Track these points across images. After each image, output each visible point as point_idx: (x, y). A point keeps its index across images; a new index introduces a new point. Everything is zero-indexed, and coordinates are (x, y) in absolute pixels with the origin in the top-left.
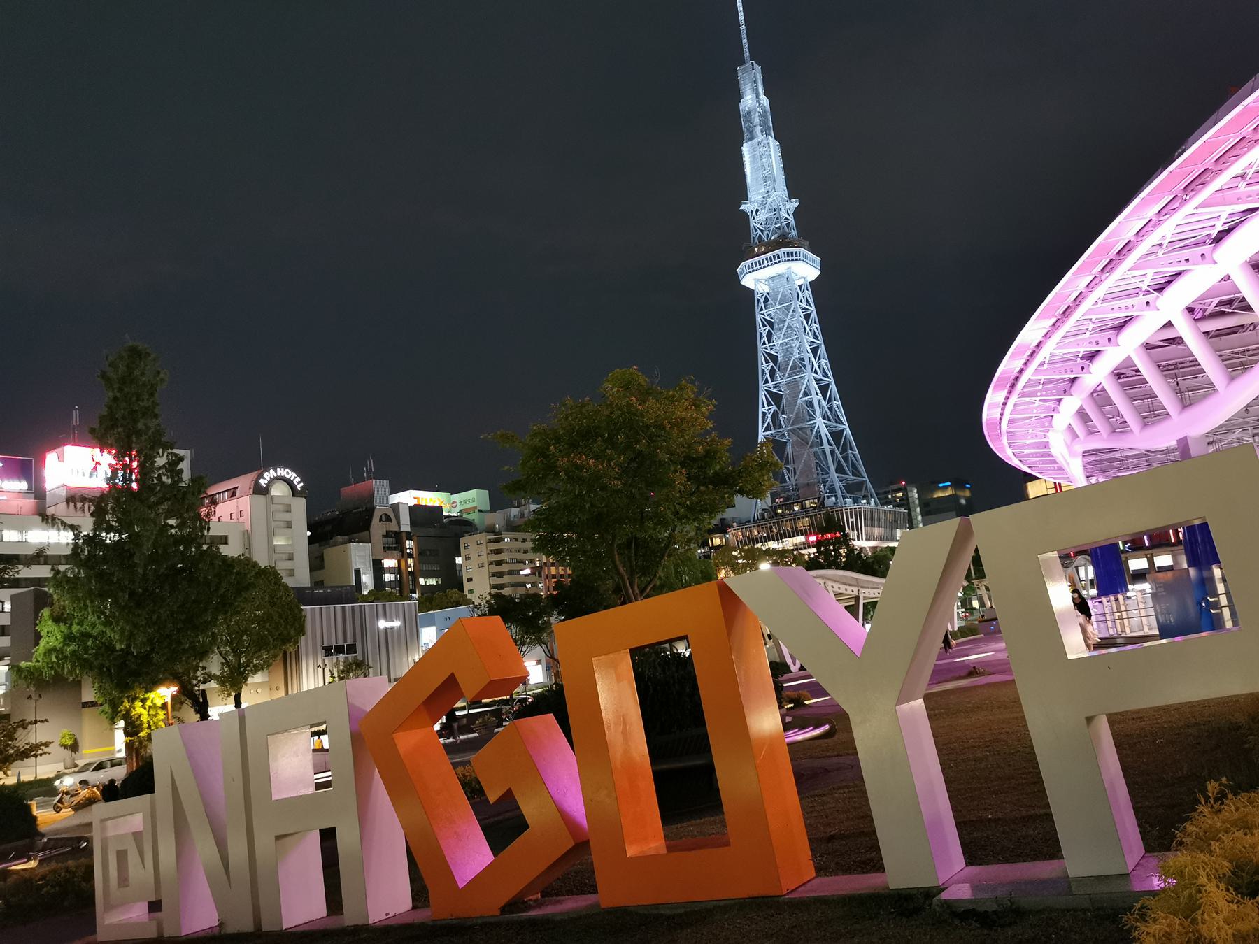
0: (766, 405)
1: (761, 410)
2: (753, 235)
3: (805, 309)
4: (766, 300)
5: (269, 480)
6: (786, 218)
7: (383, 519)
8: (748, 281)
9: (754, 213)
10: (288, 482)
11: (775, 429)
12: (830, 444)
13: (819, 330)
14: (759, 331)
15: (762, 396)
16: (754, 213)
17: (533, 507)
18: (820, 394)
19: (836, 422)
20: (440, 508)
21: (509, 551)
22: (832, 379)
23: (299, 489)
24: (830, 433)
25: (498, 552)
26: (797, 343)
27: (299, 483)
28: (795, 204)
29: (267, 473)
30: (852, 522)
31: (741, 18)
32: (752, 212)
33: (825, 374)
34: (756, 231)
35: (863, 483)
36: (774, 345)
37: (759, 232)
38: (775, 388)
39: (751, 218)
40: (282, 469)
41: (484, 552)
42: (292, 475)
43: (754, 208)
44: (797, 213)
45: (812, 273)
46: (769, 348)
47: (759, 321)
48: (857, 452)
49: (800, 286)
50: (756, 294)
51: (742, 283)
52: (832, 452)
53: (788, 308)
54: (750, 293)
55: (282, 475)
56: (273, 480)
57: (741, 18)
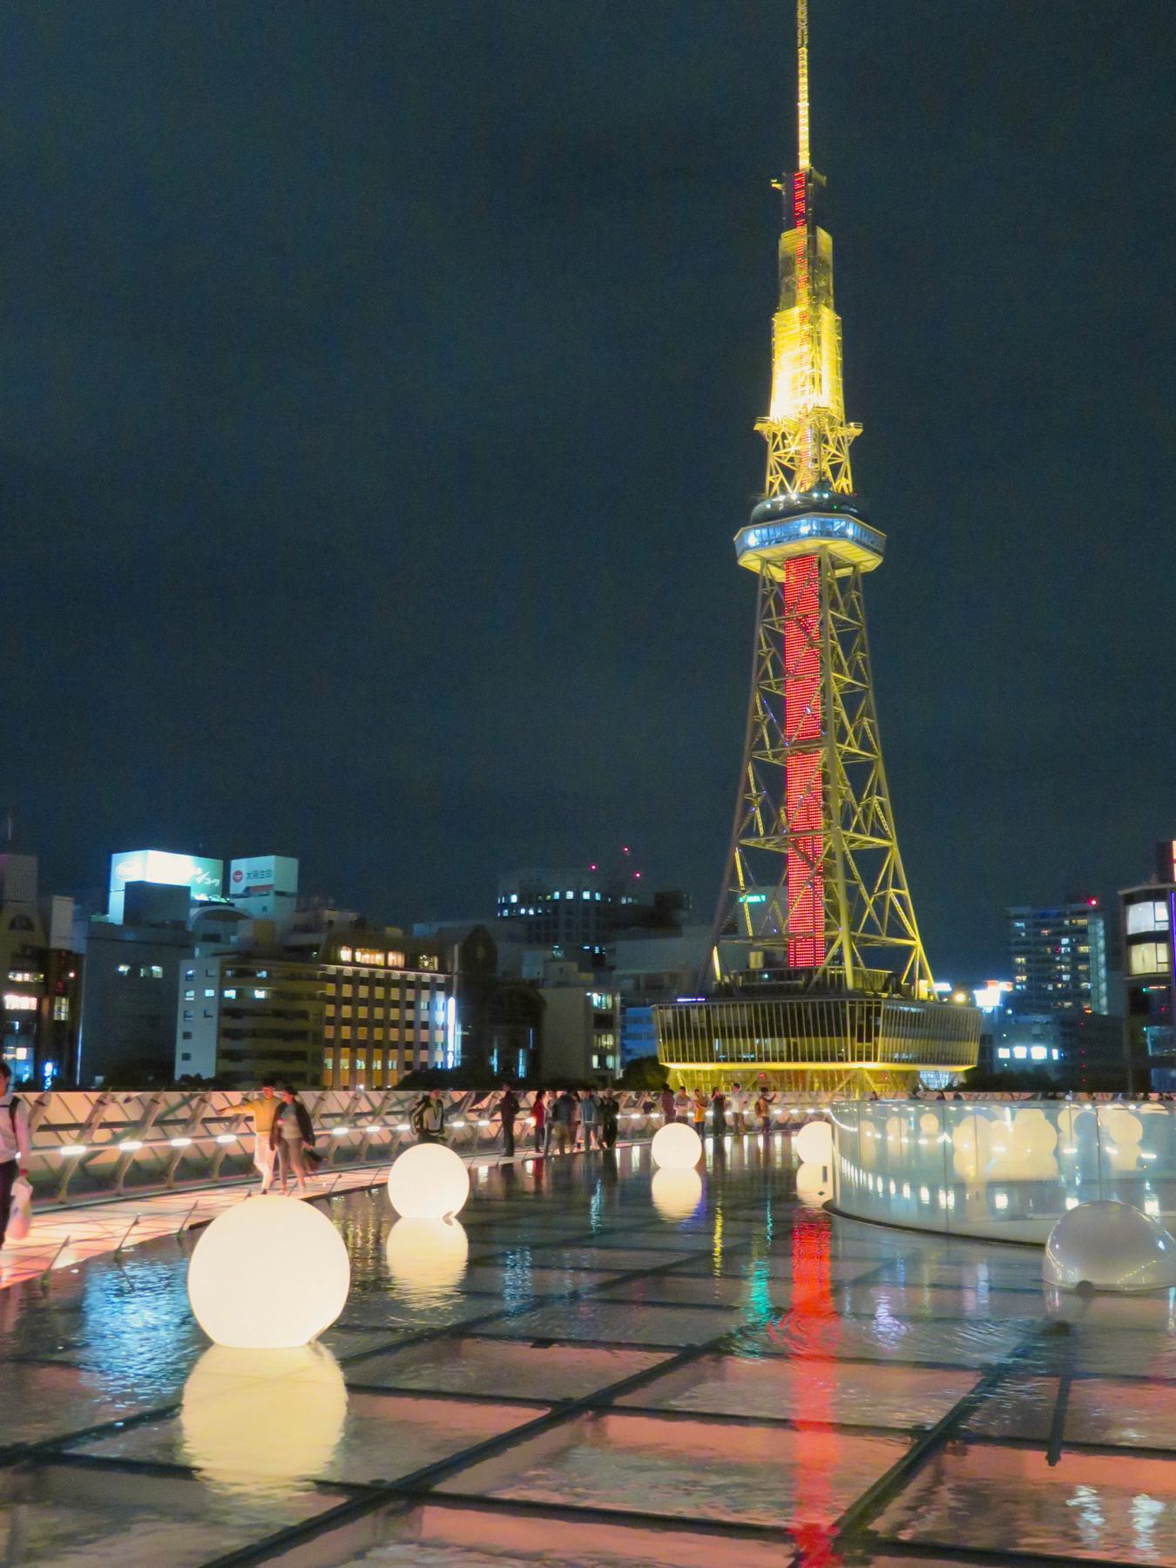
2: (769, 478)
6: (834, 455)
8: (750, 562)
9: (779, 438)
12: (848, 873)
14: (757, 652)
16: (779, 438)
19: (872, 835)
20: (185, 891)
22: (880, 753)
24: (853, 853)
26: (821, 682)
28: (854, 430)
30: (861, 1028)
32: (775, 436)
33: (865, 745)
34: (777, 473)
35: (910, 949)
37: (781, 476)
38: (775, 756)
39: (771, 448)
43: (779, 430)
44: (857, 447)
45: (870, 561)
46: (774, 686)
47: (760, 632)
48: (906, 893)
49: (843, 582)
50: (760, 583)
51: (742, 562)
52: (852, 892)
54: (751, 577)
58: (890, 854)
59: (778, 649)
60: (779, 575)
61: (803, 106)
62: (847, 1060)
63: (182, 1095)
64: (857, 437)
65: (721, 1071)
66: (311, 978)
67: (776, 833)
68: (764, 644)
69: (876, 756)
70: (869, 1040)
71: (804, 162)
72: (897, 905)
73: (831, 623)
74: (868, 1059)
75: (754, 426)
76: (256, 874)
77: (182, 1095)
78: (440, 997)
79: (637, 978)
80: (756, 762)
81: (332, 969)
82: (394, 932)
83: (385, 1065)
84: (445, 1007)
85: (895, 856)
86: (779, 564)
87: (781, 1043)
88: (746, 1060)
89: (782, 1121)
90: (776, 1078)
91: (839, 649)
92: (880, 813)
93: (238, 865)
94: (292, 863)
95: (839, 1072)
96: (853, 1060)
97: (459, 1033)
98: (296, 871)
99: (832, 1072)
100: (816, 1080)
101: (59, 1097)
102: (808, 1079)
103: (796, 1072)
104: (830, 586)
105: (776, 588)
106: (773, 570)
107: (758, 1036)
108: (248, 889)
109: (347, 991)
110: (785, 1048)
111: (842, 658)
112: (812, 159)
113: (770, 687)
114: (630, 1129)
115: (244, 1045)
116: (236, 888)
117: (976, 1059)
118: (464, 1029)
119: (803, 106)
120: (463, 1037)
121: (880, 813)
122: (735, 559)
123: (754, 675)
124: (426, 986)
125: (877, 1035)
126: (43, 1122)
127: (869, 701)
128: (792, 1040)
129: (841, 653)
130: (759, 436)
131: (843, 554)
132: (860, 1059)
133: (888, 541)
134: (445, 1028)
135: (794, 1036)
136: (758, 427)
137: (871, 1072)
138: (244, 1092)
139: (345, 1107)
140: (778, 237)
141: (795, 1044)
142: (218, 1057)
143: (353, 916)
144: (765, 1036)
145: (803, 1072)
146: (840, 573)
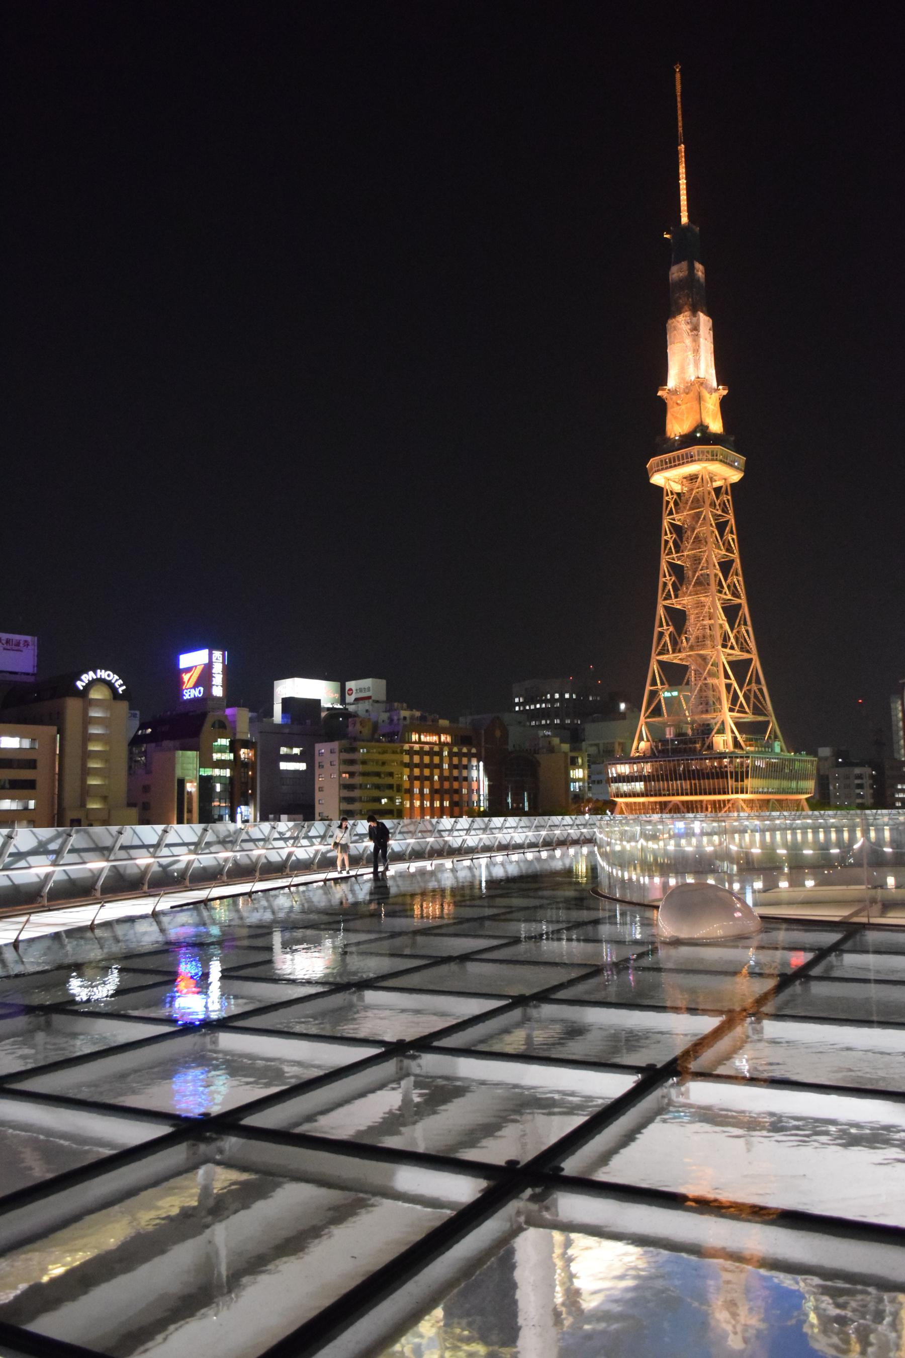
0: (664, 624)
1: (657, 629)
3: (720, 515)
4: (676, 503)
5: (87, 682)
7: (217, 726)
8: (658, 479)
10: (109, 685)
11: (674, 652)
12: (727, 676)
13: (736, 541)
15: (661, 612)
17: (405, 713)
18: (724, 618)
20: (318, 702)
21: (364, 762)
23: (121, 692)
24: (729, 663)
25: (352, 762)
27: (121, 686)
29: (85, 675)
31: (682, 170)
33: (735, 594)
36: (683, 556)
40: (103, 671)
41: (336, 763)
42: (113, 678)
45: (735, 476)
49: (718, 490)
52: (728, 687)
53: (697, 516)
54: (659, 490)
55: (103, 677)
56: (91, 683)
57: (682, 170)
58: (753, 662)
59: (677, 535)
60: (677, 488)
61: (683, 182)
62: (728, 794)
63: (57, 830)
64: (724, 396)
65: (649, 802)
66: (394, 752)
67: (680, 651)
68: (668, 532)
69: (743, 601)
70: (742, 780)
71: (684, 220)
72: (758, 693)
73: (711, 516)
74: (742, 792)
75: (657, 393)
76: (361, 690)
77: (57, 830)
78: (474, 762)
79: (597, 745)
80: (666, 607)
81: (406, 747)
82: (444, 723)
83: (442, 804)
84: (478, 767)
85: (756, 663)
86: (677, 480)
87: (686, 783)
88: (665, 795)
89: (562, 839)
90: (683, 805)
91: (717, 533)
92: (747, 637)
93: (350, 685)
94: (383, 682)
95: (724, 801)
96: (732, 793)
97: (486, 783)
98: (385, 687)
99: (719, 801)
100: (709, 806)
101: (107, 830)
102: (704, 806)
103: (696, 801)
104: (709, 493)
105: (675, 496)
106: (672, 483)
107: (672, 780)
108: (356, 700)
109: (416, 759)
110: (689, 787)
111: (719, 538)
112: (689, 217)
113: (674, 559)
114: (555, 839)
115: (356, 793)
116: (350, 699)
117: (813, 791)
118: (489, 780)
119: (683, 182)
120: (489, 786)
121: (747, 637)
122: (648, 479)
123: (662, 552)
124: (465, 755)
125: (747, 777)
126: (15, 851)
127: (737, 564)
128: (693, 782)
129: (718, 535)
130: (659, 396)
131: (718, 472)
132: (737, 793)
133: (746, 461)
134: (478, 780)
135: (694, 779)
136: (660, 393)
137: (744, 801)
138: (272, 823)
139: (266, 835)
140: (669, 268)
141: (695, 784)
142: (340, 802)
143: (418, 714)
144: (676, 780)
145: (701, 801)
146: (717, 484)
